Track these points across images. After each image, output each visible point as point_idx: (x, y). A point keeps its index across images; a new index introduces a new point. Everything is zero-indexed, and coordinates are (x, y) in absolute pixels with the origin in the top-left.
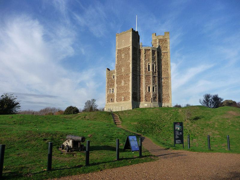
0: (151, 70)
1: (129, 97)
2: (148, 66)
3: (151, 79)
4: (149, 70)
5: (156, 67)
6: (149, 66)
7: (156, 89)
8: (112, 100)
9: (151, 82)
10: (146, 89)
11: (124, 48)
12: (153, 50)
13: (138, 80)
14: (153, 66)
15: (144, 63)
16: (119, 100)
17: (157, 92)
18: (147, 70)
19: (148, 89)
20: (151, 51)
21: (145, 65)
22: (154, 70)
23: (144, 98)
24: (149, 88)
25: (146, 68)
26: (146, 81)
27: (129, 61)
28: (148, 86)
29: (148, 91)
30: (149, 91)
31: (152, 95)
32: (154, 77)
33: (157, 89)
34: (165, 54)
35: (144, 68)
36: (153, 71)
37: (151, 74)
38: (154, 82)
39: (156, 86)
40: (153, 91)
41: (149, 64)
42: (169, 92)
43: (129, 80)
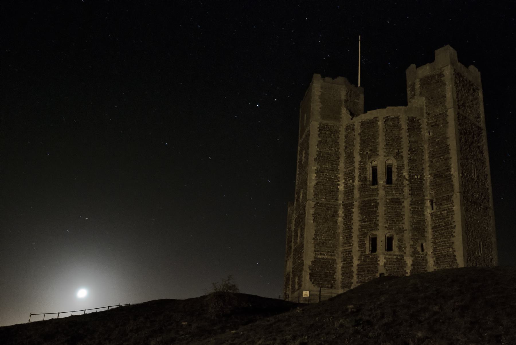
0: (381, 182)
4: (375, 181)
7: (400, 241)
10: (362, 244)
13: (340, 219)
15: (357, 165)
17: (408, 250)
21: (363, 169)
22: (394, 178)
23: (355, 277)
25: (363, 180)
26: (362, 221)
29: (368, 252)
30: (374, 249)
35: (357, 179)
36: (389, 181)
37: (382, 192)
38: (395, 217)
39: (401, 231)
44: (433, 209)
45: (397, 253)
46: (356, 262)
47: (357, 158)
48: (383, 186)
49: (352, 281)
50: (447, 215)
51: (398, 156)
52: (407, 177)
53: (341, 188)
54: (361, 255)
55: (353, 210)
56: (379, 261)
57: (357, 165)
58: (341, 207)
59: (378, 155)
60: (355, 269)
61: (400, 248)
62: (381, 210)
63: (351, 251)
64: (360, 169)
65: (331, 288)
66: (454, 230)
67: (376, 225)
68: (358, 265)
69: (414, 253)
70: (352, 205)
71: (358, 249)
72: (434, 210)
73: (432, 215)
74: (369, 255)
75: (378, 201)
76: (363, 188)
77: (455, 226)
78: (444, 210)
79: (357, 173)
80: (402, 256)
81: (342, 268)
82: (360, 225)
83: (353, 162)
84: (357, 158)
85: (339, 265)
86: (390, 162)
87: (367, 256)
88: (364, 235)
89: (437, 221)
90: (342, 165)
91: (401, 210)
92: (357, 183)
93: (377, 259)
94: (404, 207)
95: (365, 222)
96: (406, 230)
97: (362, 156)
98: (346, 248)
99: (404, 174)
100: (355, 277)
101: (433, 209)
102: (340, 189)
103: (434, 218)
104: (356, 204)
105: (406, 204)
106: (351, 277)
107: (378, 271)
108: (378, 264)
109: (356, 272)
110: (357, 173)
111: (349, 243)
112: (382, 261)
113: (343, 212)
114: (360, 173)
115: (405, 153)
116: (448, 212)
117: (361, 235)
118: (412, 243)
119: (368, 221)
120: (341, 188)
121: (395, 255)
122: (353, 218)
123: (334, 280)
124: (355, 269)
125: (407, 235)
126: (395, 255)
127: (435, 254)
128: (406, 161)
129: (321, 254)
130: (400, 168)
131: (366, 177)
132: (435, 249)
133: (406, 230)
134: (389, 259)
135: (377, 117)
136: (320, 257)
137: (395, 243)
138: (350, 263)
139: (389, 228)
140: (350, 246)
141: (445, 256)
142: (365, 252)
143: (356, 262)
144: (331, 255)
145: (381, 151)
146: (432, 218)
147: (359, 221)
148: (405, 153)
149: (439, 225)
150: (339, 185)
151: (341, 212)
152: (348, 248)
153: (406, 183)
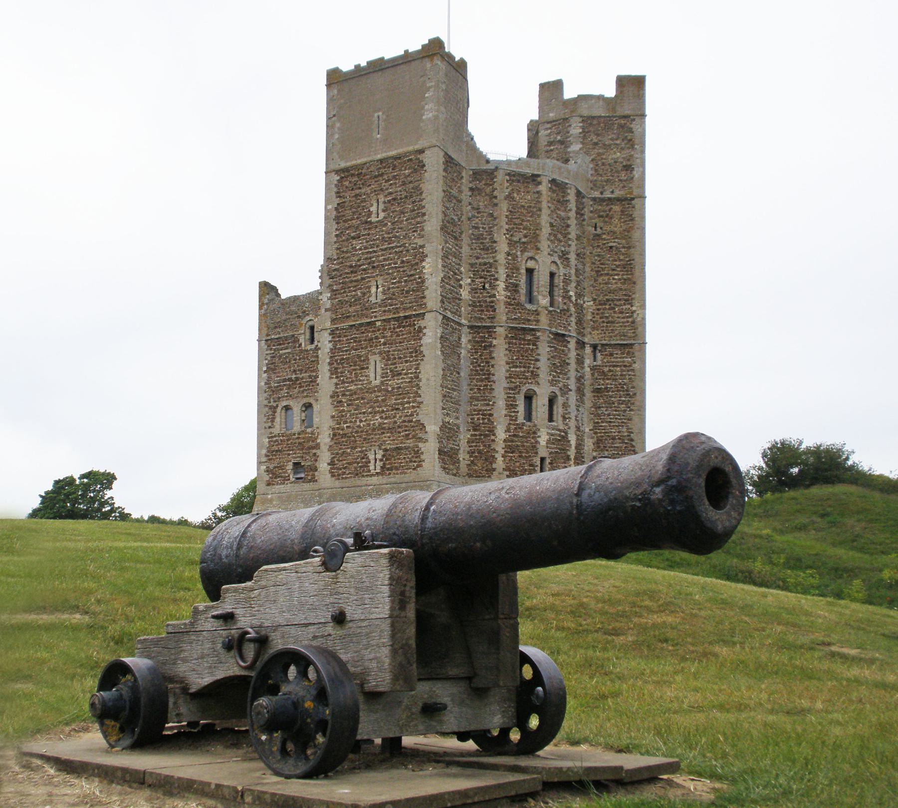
0: (544, 301)
1: (418, 453)
2: (523, 271)
3: (544, 349)
5: (567, 281)
6: (530, 272)
8: (304, 471)
9: (543, 364)
10: (511, 406)
11: (381, 161)
12: (553, 181)
14: (552, 275)
15: (501, 257)
16: (350, 467)
17: (572, 424)
18: (523, 298)
19: (521, 408)
20: (544, 188)
21: (513, 268)
23: (500, 459)
24: (529, 398)
25: (513, 288)
27: (420, 242)
28: (524, 389)
29: (521, 419)
30: (529, 416)
31: (543, 439)
32: (560, 338)
33: (573, 408)
34: (617, 208)
35: (501, 285)
37: (544, 319)
39: (565, 390)
40: (551, 419)
41: (531, 264)
42: (634, 425)
43: (417, 353)
44: (595, 360)
45: (561, 427)
46: (501, 434)
47: (503, 247)
48: (546, 308)
49: (494, 466)
50: (621, 375)
51: (564, 256)
52: (574, 299)
53: (465, 294)
54: (510, 424)
55: (495, 342)
56: (539, 437)
57: (501, 257)
58: (465, 330)
59: (538, 249)
60: (500, 447)
61: (564, 418)
62: (544, 349)
63: (491, 415)
64: (507, 268)
65: (455, 475)
66: (632, 400)
67: (535, 375)
68: (505, 441)
69: (578, 428)
70: (490, 330)
71: (504, 412)
72: (599, 363)
73: (593, 369)
74: (523, 424)
75: (538, 334)
76: (513, 304)
77: (635, 394)
78: (617, 366)
79: (502, 273)
80: (566, 433)
81: (468, 442)
82: (507, 371)
83: (489, 248)
84: (503, 247)
85: (464, 437)
86: (553, 268)
87: (520, 427)
88: (516, 389)
89: (602, 382)
90: (465, 250)
91: (566, 355)
92: (501, 292)
93: (535, 433)
94: (569, 350)
95: (517, 367)
96: (571, 390)
97: (511, 244)
98: (479, 407)
99: (571, 293)
100: (500, 459)
101: (595, 360)
102: (463, 297)
103: (596, 375)
104: (500, 331)
105: (572, 345)
106: (491, 459)
107: (537, 453)
108: (537, 442)
109: (503, 452)
110: (502, 273)
111: (485, 400)
112: (543, 439)
113: (469, 341)
114: (507, 276)
115: (572, 257)
116: (622, 371)
117: (510, 389)
118: (575, 413)
119: (520, 367)
120: (465, 294)
121: (559, 430)
122: (494, 355)
123: (458, 462)
124: (500, 447)
125: (573, 397)
126: (559, 430)
127: (596, 433)
128: (573, 271)
129: (448, 414)
130: (567, 281)
131: (516, 286)
132: (596, 426)
133: (571, 390)
134: (552, 435)
135: (538, 176)
136: (447, 420)
137: (558, 410)
138: (486, 436)
139: (552, 383)
140: (488, 405)
141: (614, 438)
142: (516, 420)
143: (501, 434)
144: (457, 418)
145: (544, 244)
146: (593, 375)
147: (508, 363)
148: (572, 257)
149: (606, 388)
150: (461, 286)
151: (464, 340)
152: (484, 408)
153: (573, 309)
